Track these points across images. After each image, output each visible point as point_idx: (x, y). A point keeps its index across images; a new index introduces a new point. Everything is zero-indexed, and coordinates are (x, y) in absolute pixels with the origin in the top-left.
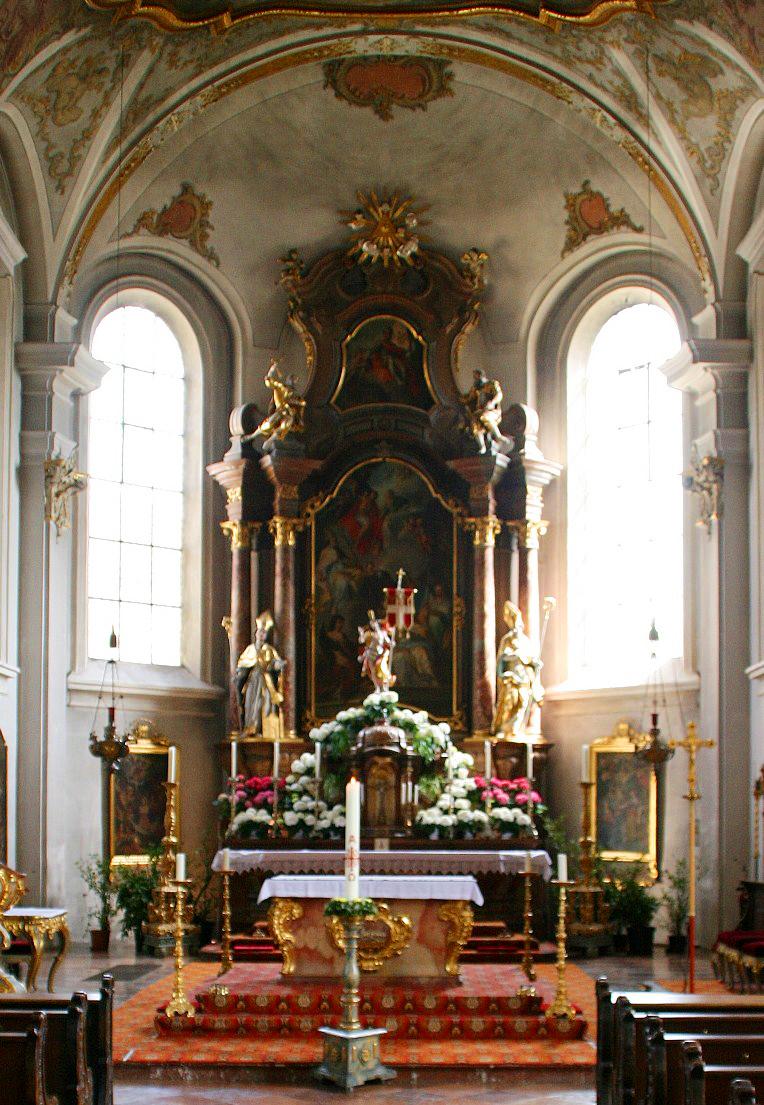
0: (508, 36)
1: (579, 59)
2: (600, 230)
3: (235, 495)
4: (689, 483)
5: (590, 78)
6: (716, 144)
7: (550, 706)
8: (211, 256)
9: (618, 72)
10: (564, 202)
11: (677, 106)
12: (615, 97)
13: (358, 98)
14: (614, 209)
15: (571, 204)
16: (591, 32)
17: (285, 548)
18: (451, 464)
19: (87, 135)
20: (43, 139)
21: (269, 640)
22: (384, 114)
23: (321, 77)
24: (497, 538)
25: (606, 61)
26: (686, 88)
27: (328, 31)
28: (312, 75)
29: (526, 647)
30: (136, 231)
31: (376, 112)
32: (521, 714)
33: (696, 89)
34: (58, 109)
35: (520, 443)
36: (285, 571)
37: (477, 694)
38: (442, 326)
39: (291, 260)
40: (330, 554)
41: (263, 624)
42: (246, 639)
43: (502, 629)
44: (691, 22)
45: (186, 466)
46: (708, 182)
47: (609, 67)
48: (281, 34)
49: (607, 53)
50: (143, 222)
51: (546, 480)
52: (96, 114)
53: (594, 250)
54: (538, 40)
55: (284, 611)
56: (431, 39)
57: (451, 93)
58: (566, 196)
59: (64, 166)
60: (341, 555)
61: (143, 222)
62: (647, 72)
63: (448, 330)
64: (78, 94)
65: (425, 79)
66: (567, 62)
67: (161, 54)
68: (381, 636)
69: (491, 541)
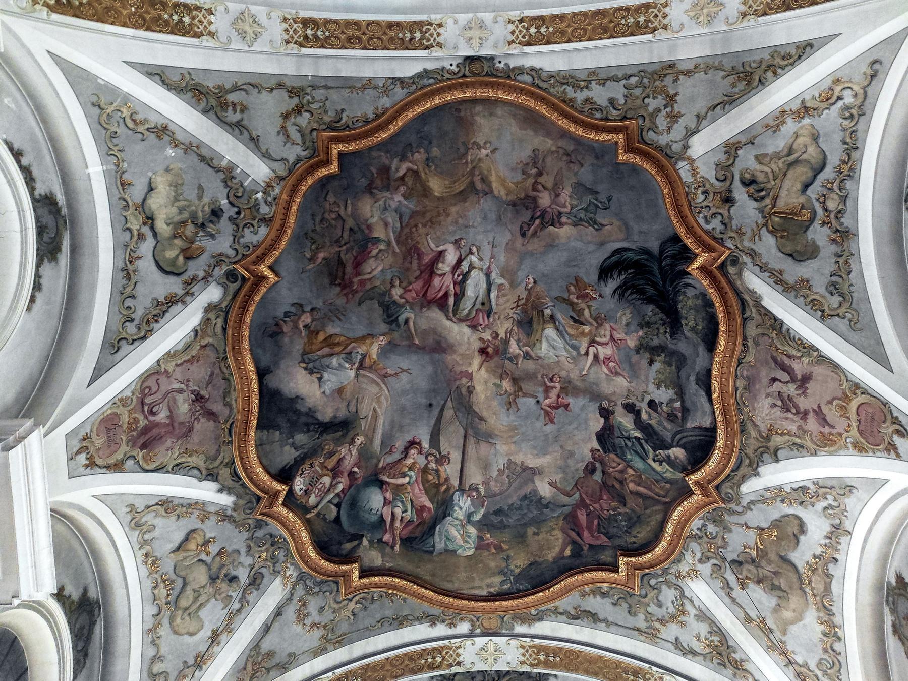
0: (593, 618)
1: (663, 622)
5: (678, 646)
6: (825, 651)
9: (704, 616)
11: (770, 623)
12: (704, 656)
16: (665, 572)
20: (153, 643)
25: (688, 607)
26: (774, 588)
27: (441, 630)
33: (783, 583)
34: (180, 608)
44: (757, 474)
47: (692, 612)
48: (400, 622)
49: (687, 594)
52: (215, 638)
54: (619, 614)
56: (528, 640)
62: (727, 587)
64: (202, 599)
66: (651, 635)
67: (292, 594)
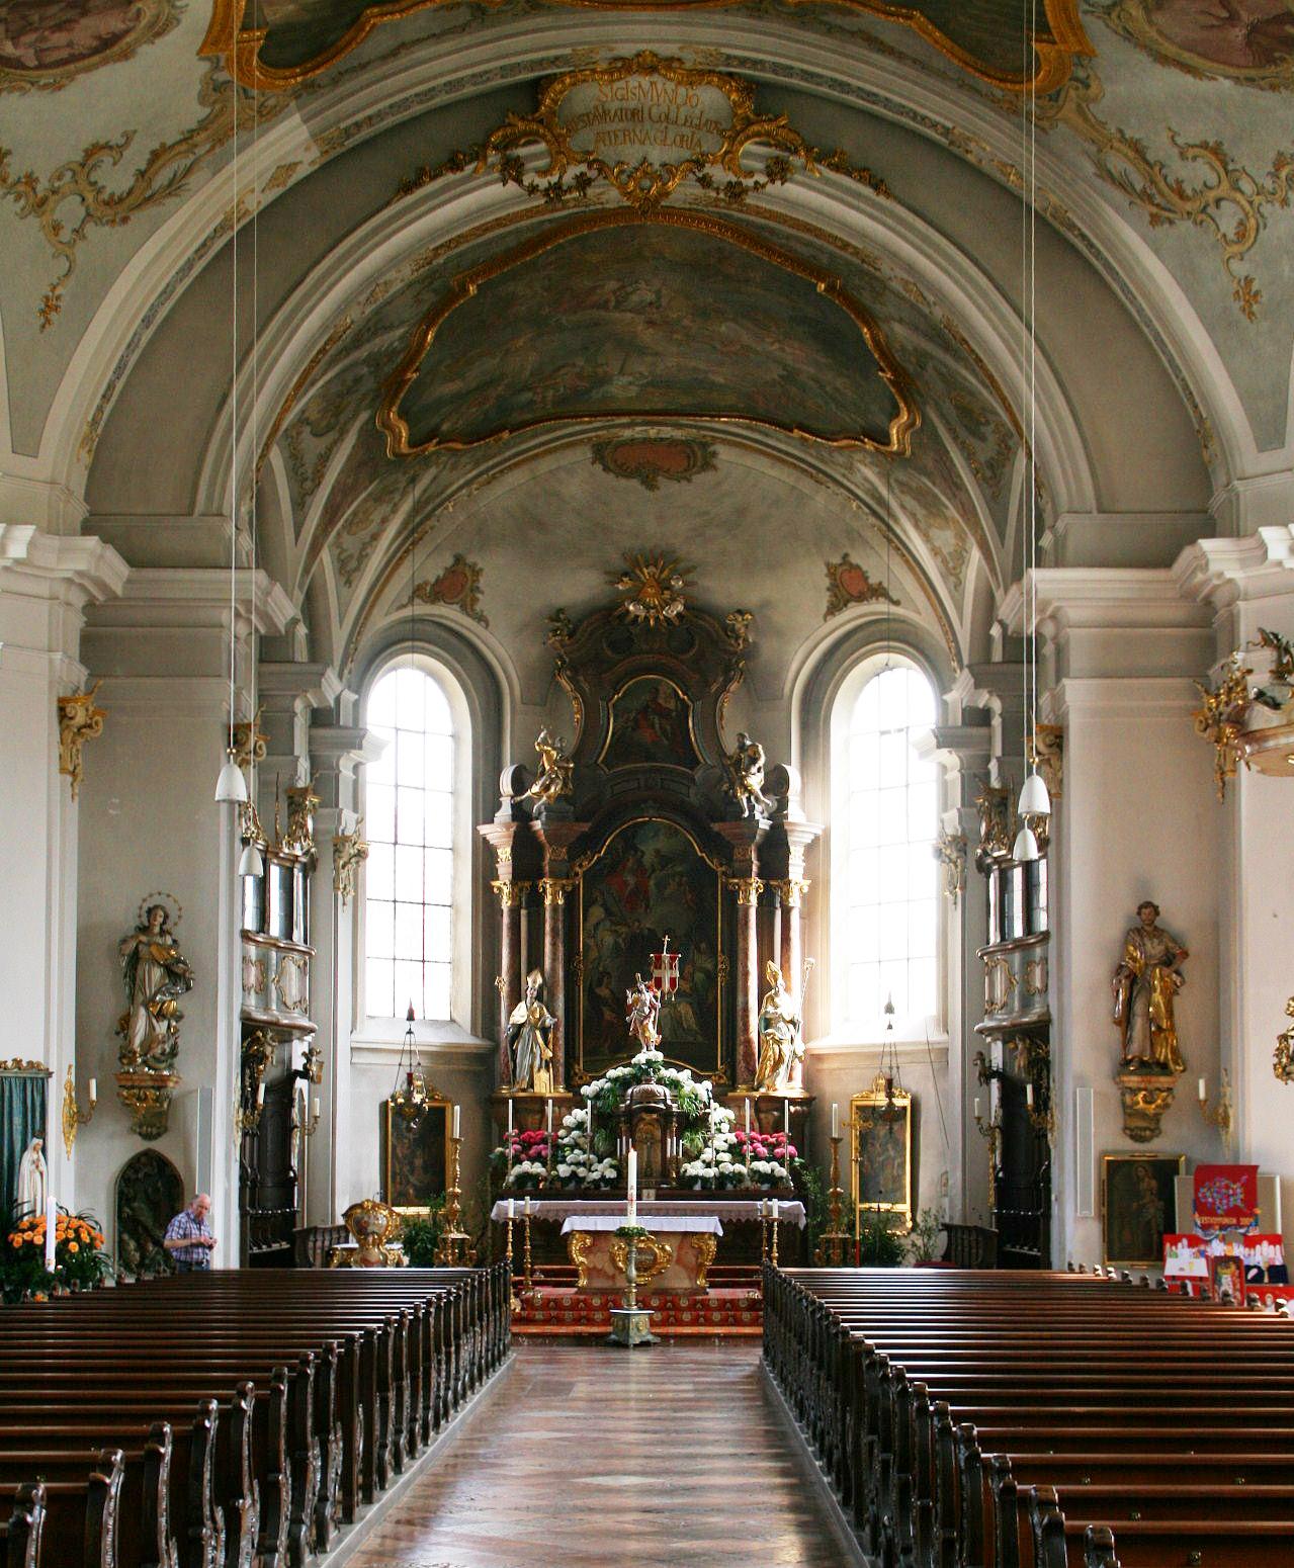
2: (861, 598)
3: (505, 853)
4: (939, 853)
7: (812, 1061)
8: (481, 618)
9: (866, 479)
10: (825, 571)
13: (623, 471)
14: (873, 580)
15: (832, 572)
17: (555, 907)
18: (716, 827)
19: (375, 537)
21: (539, 998)
22: (650, 484)
23: (589, 455)
24: (760, 898)
28: (584, 454)
29: (788, 1004)
30: (411, 600)
31: (643, 483)
32: (782, 1069)
35: (783, 804)
36: (554, 930)
37: (741, 1049)
38: (708, 685)
39: (558, 620)
40: (597, 912)
41: (533, 981)
42: (516, 996)
43: (764, 988)
45: (456, 824)
46: (952, 579)
50: (418, 592)
51: (808, 839)
52: (384, 521)
53: (853, 615)
55: (554, 969)
57: (715, 468)
58: (828, 565)
59: (353, 564)
60: (608, 912)
61: (418, 592)
63: (714, 688)
65: (695, 458)
68: (648, 996)
69: (754, 899)
